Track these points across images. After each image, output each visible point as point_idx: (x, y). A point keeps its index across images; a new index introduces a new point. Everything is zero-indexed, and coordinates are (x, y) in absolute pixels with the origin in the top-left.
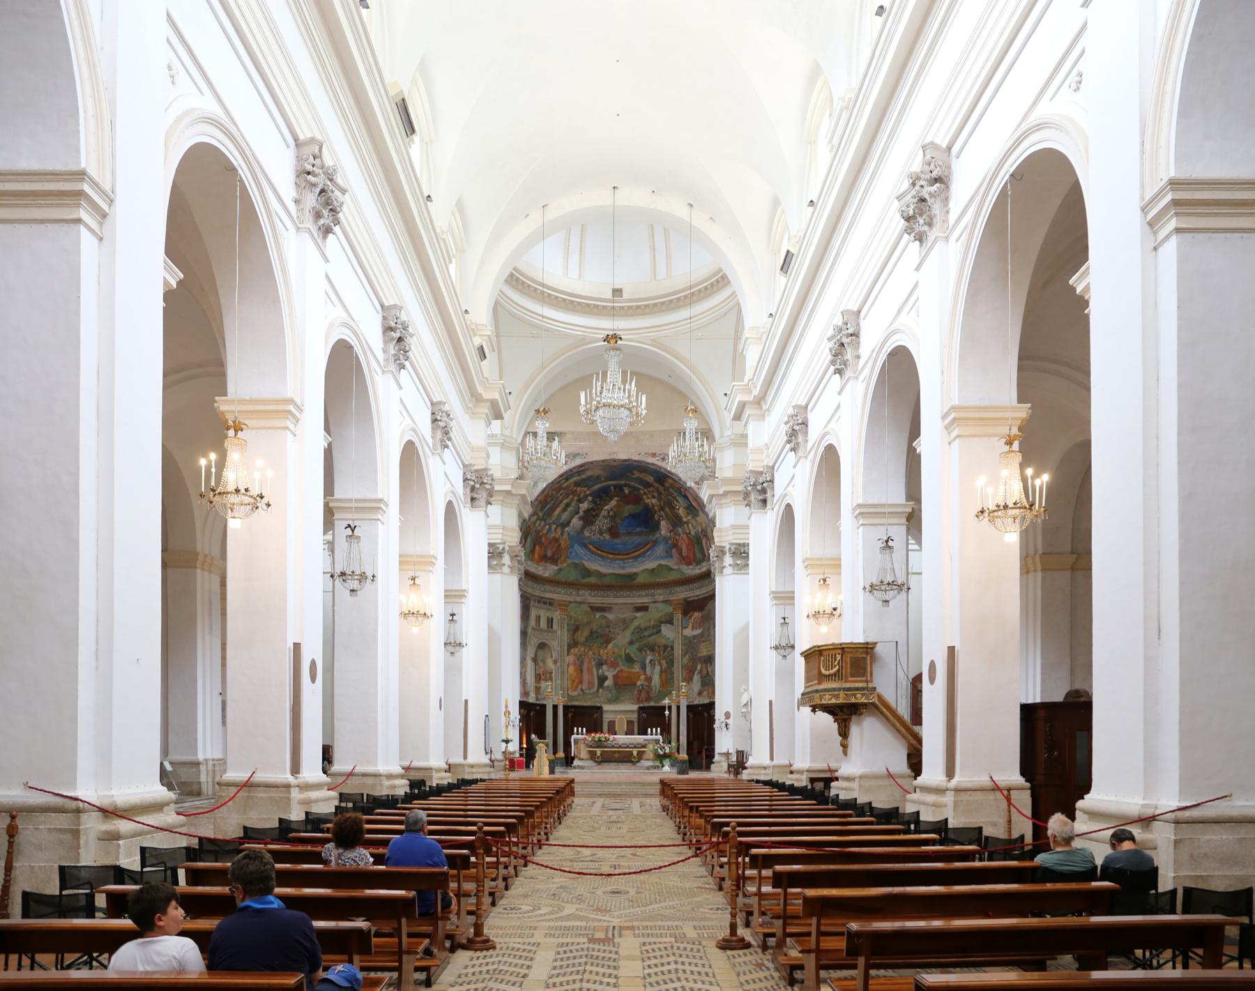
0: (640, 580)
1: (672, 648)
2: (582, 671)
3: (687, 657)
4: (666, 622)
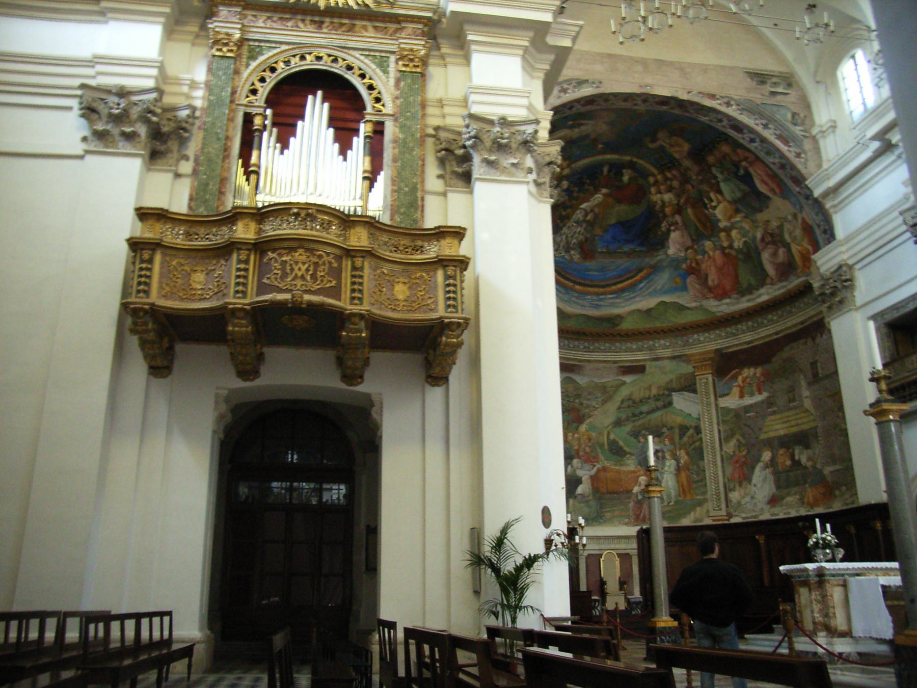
0: (626, 326)
1: (698, 430)
3: (733, 443)
4: (679, 391)
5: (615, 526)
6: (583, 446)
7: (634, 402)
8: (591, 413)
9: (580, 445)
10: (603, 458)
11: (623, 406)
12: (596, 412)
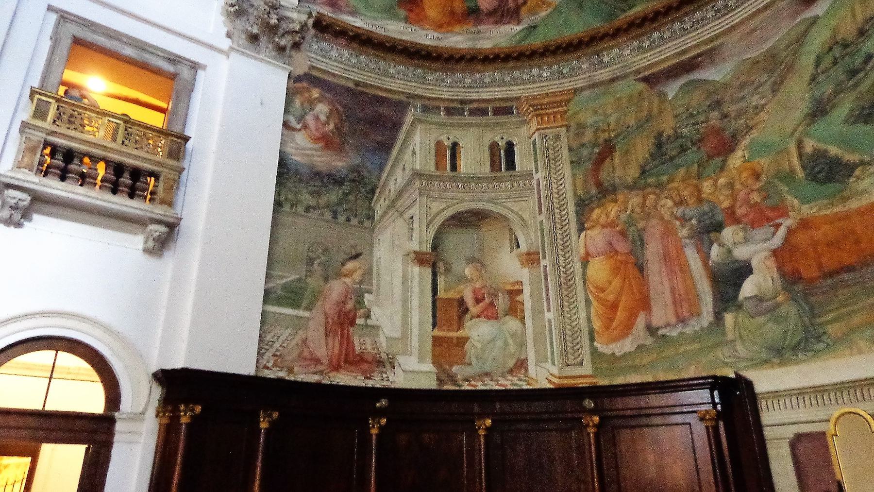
2: (641, 268)
5: (860, 352)
6: (742, 195)
7: (846, 46)
8: (751, 123)
9: (734, 197)
10: (796, 202)
11: (823, 67)
12: (763, 116)
